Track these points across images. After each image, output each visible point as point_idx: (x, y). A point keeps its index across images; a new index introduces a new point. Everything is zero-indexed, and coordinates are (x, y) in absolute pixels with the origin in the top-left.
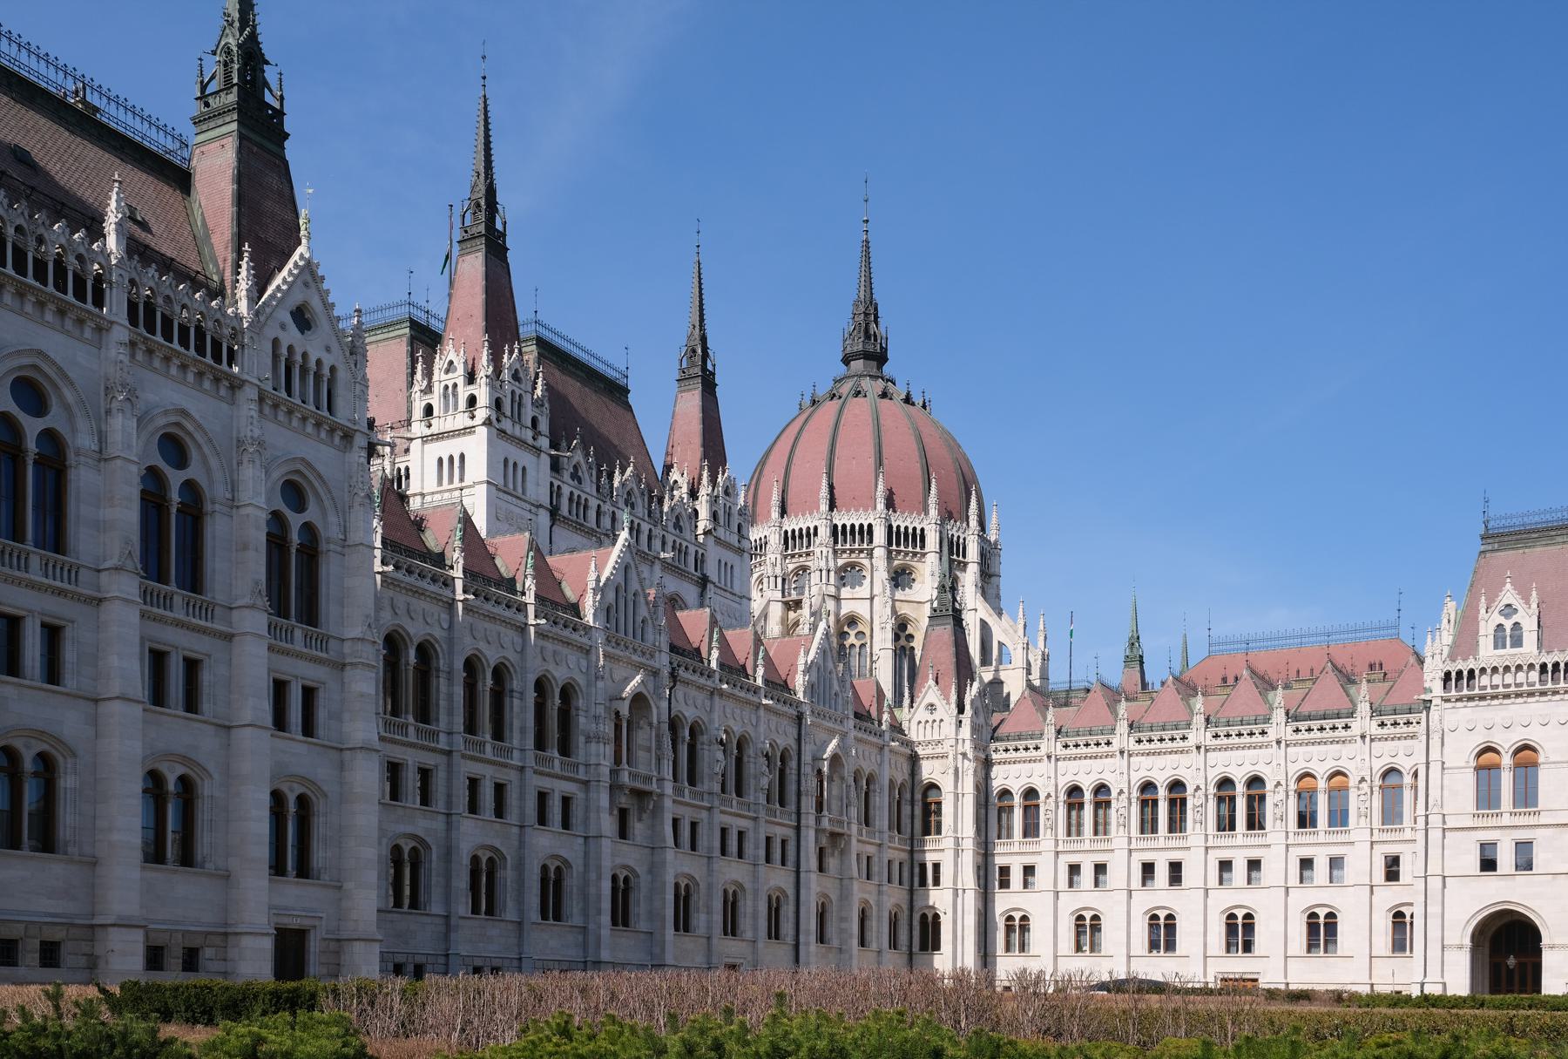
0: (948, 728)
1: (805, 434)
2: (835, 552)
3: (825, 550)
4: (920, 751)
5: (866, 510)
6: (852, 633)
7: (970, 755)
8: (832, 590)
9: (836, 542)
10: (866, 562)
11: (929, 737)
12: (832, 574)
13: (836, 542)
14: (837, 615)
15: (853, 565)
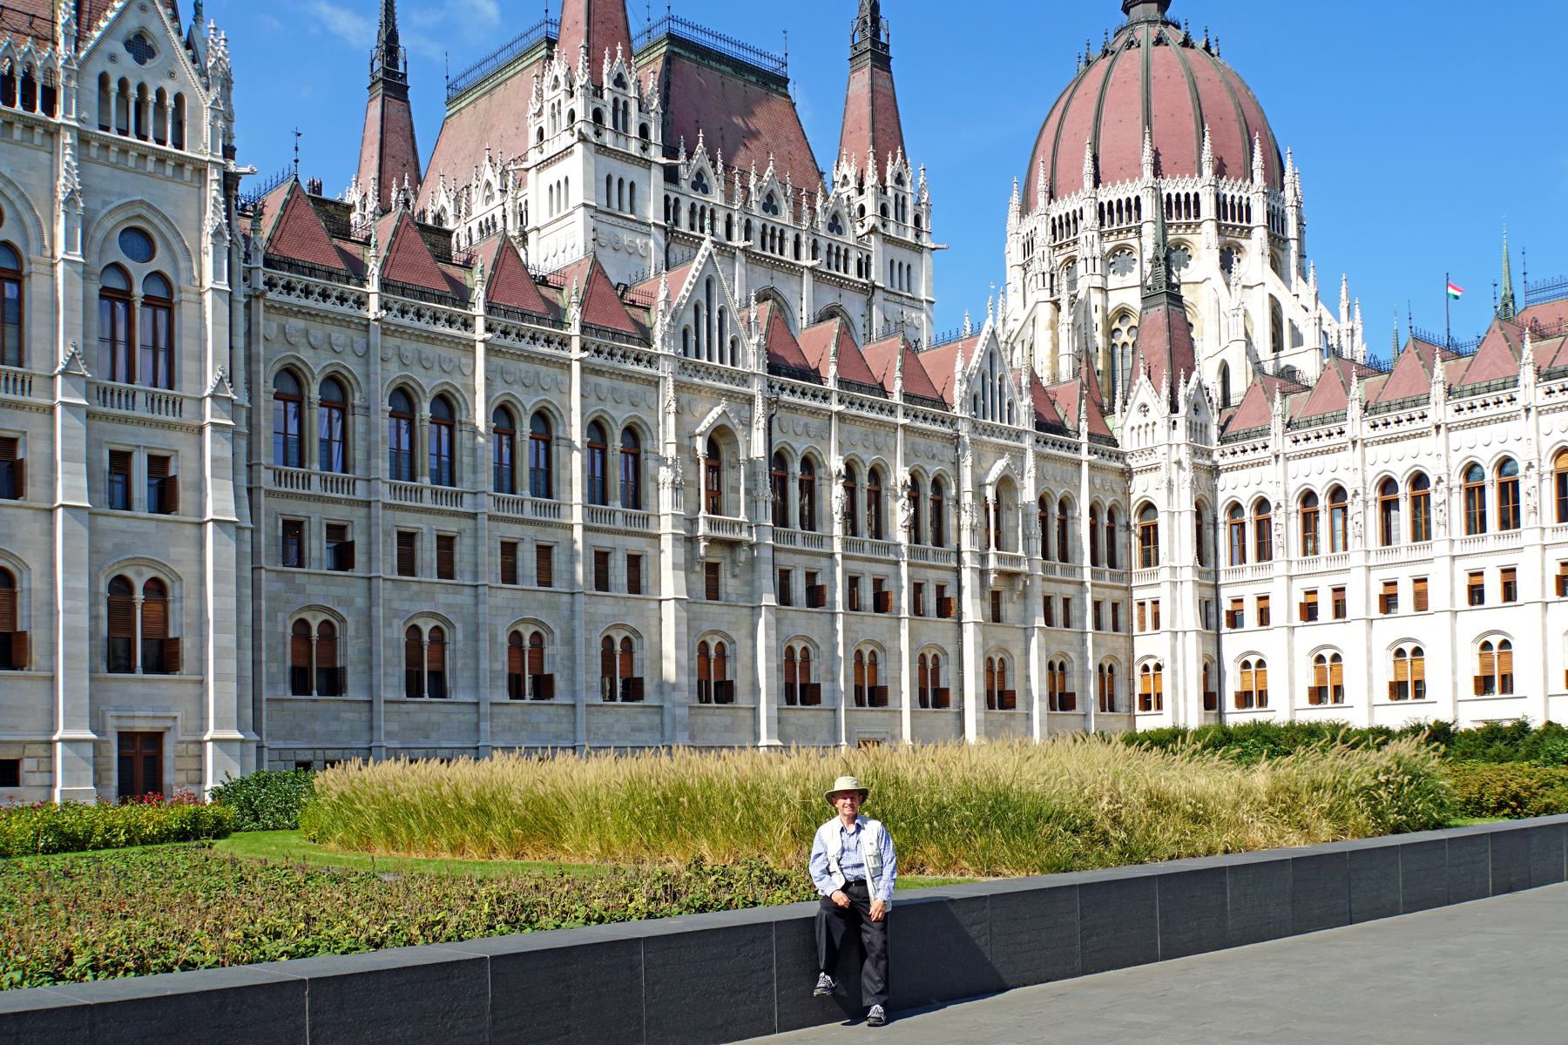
0: (1162, 431)
1: (1074, 103)
2: (1102, 235)
3: (1090, 234)
4: (1134, 464)
5: (1132, 181)
6: (1124, 329)
7: (1186, 463)
8: (1098, 281)
9: (1102, 224)
10: (1135, 243)
11: (1143, 446)
12: (1098, 262)
13: (1102, 224)
14: (1105, 309)
15: (1121, 248)
